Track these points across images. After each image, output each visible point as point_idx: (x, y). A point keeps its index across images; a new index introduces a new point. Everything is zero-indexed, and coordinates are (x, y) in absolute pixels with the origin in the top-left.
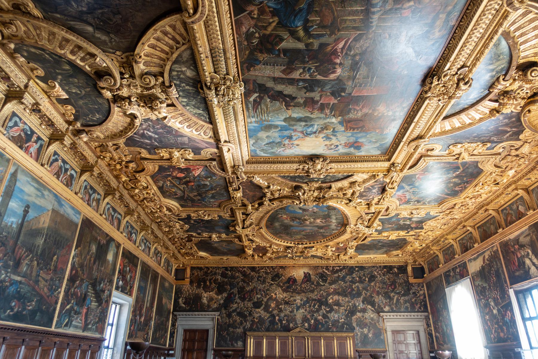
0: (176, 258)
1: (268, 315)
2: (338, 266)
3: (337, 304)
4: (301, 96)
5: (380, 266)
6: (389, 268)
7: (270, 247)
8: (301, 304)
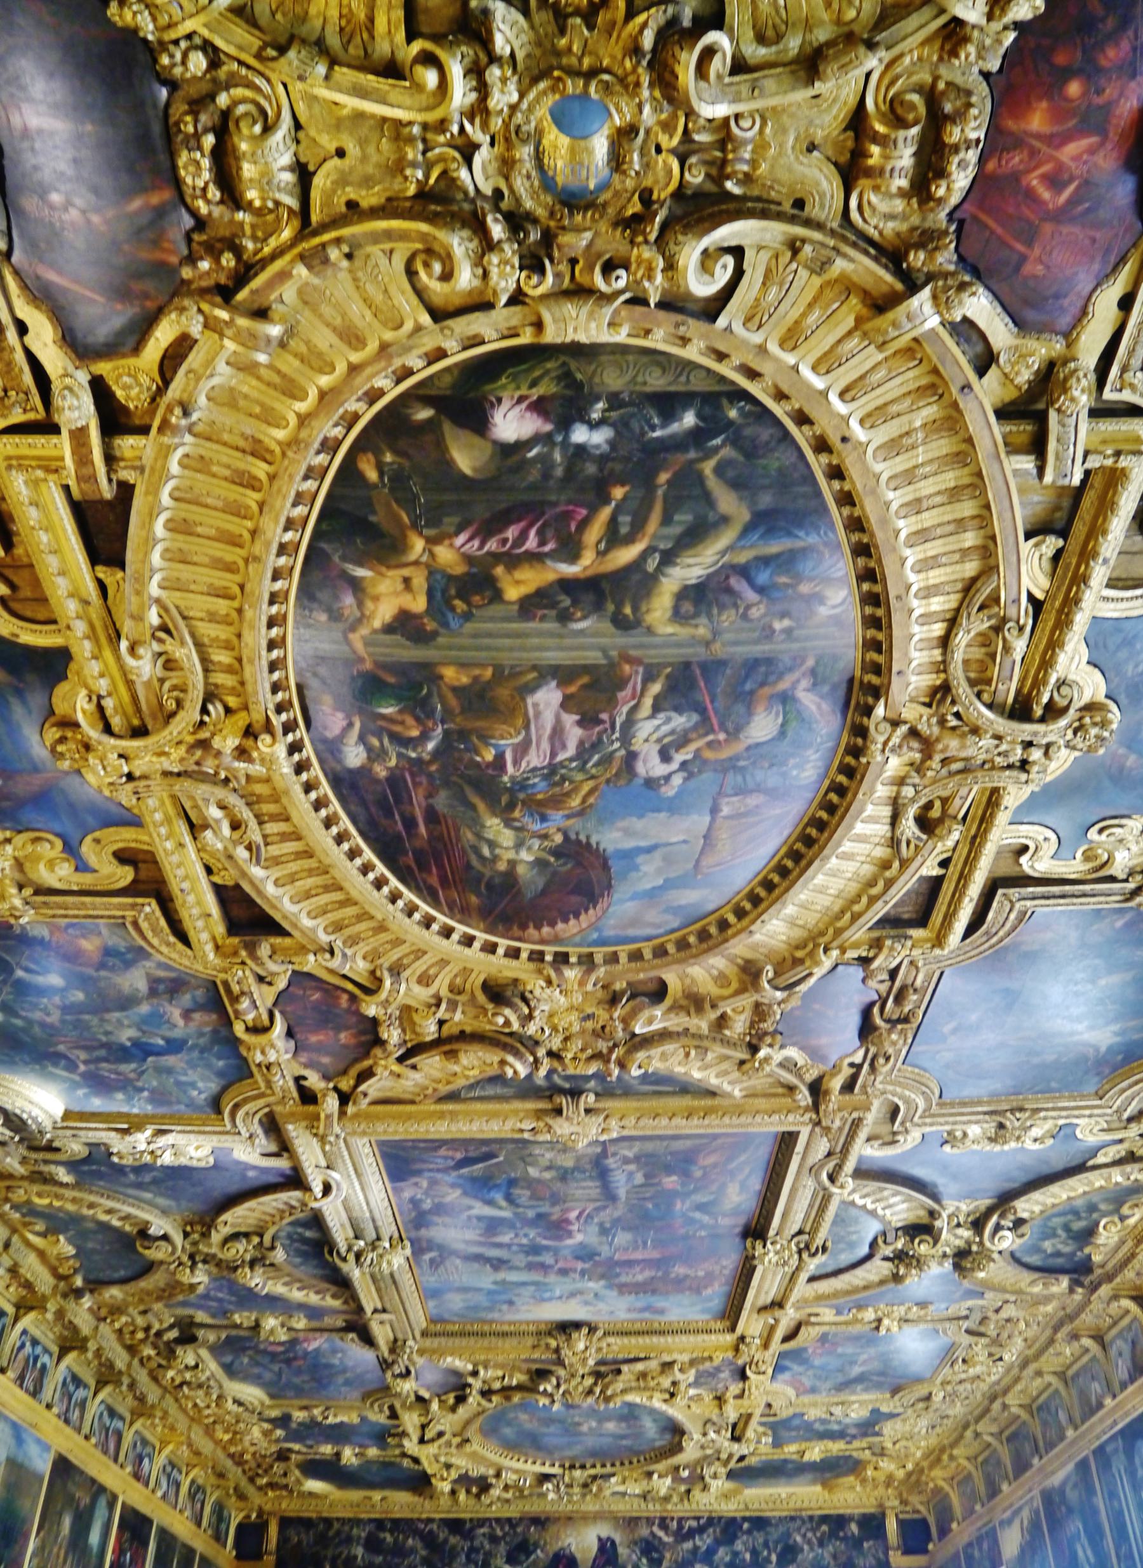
0: (241, 1496)
4: (520, 1260)
5: (811, 1518)
6: (837, 1522)
7: (498, 1475)
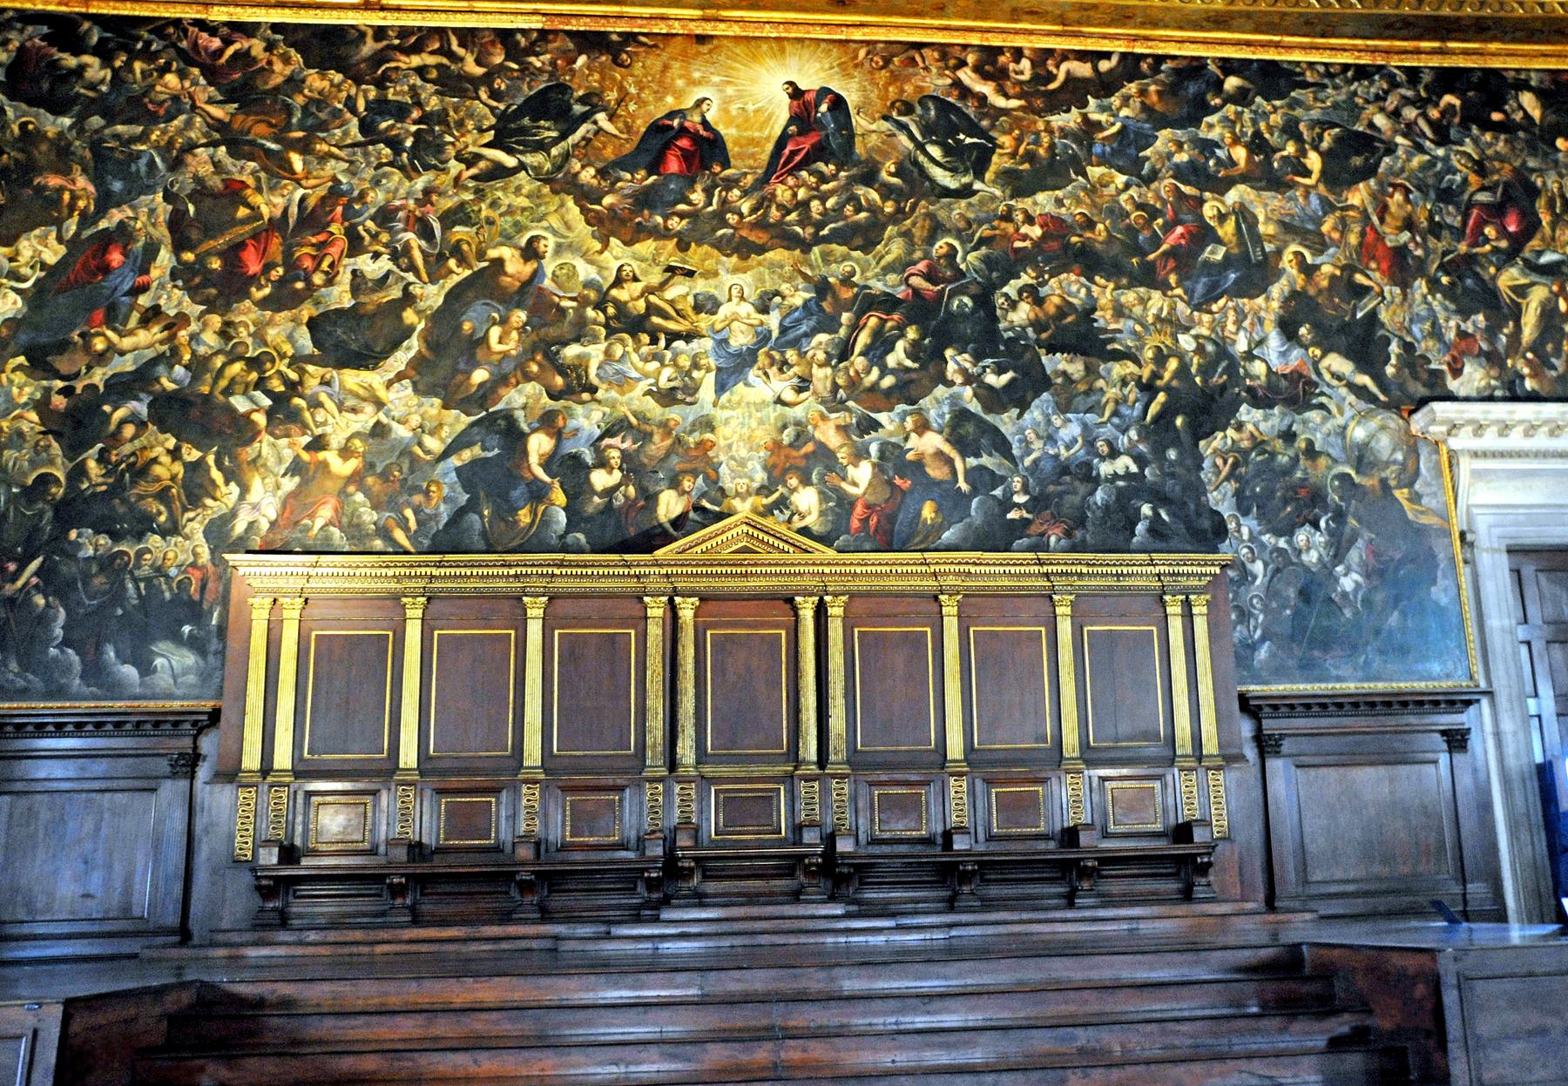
1: (457, 421)
2: (1082, 56)
3: (1081, 335)
5: (1413, 74)
8: (763, 338)
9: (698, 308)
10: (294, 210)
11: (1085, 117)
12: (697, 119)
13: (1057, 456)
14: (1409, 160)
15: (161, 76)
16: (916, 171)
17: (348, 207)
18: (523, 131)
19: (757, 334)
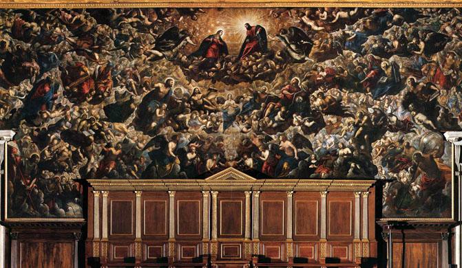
2: (345, 9)
3: (336, 109)
8: (237, 111)
9: (218, 102)
10: (97, 72)
11: (344, 32)
12: (218, 38)
13: (326, 148)
14: (456, 43)
15: (55, 28)
16: (286, 54)
17: (112, 71)
18: (164, 44)
19: (236, 110)
